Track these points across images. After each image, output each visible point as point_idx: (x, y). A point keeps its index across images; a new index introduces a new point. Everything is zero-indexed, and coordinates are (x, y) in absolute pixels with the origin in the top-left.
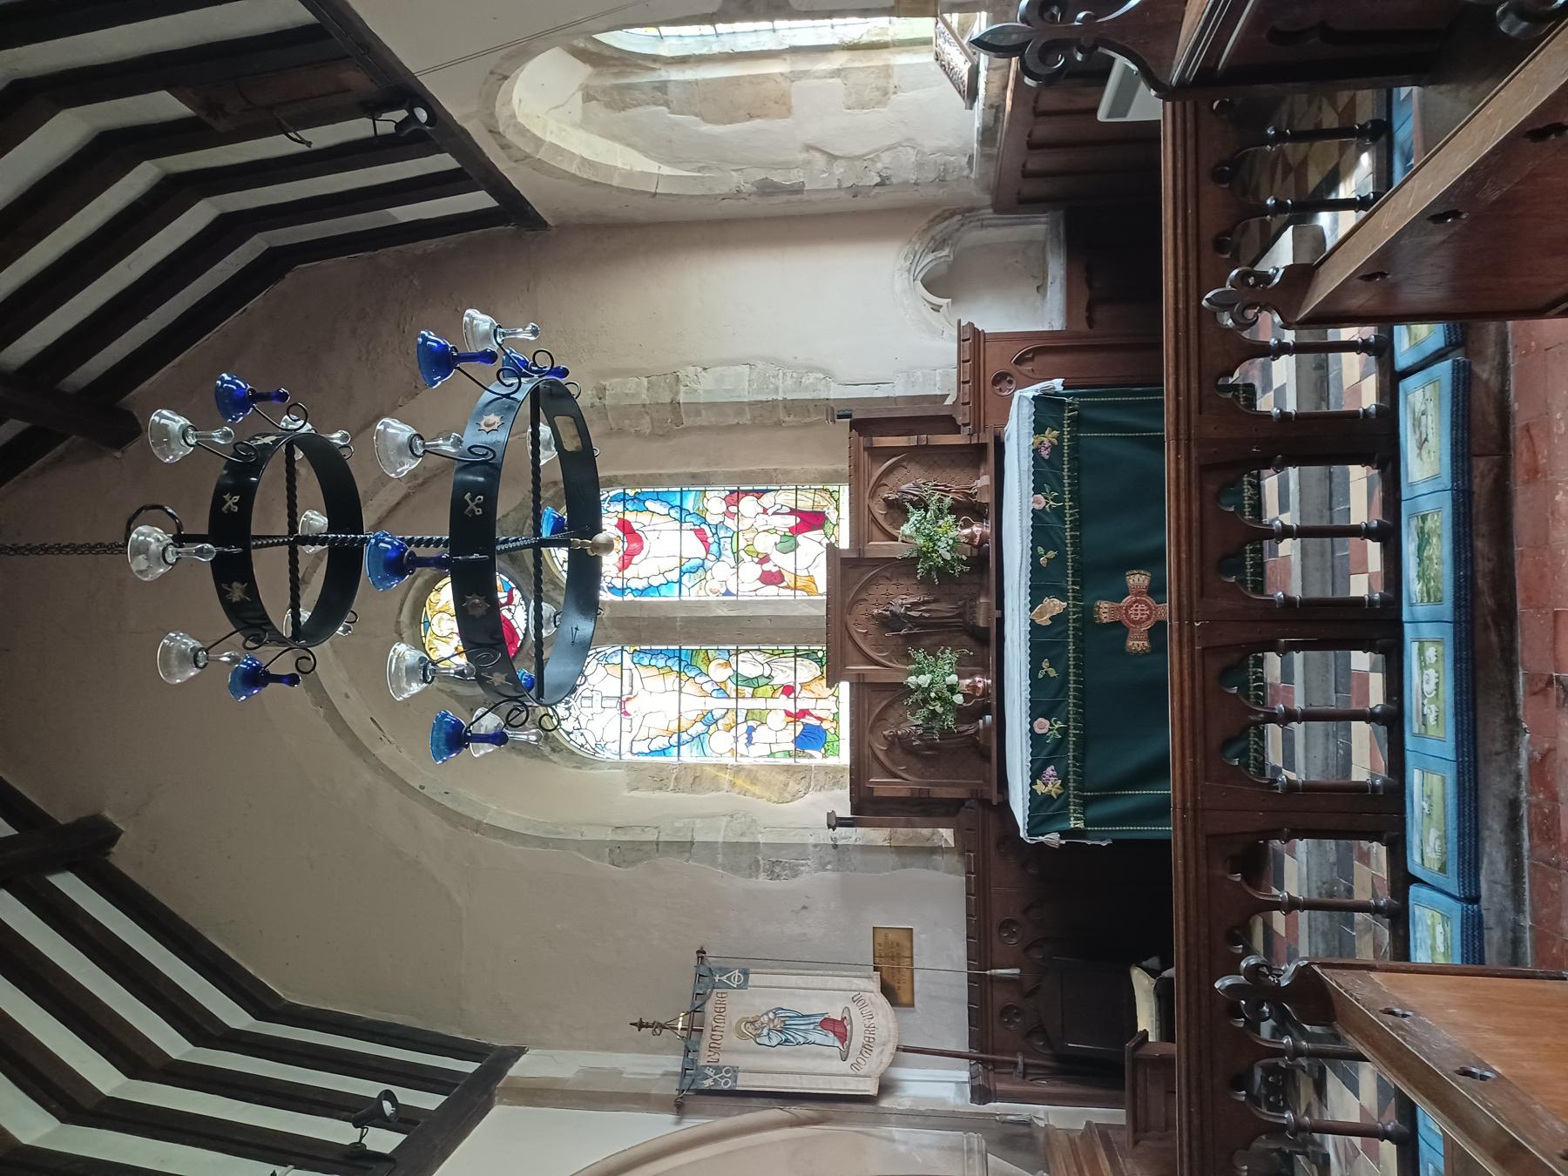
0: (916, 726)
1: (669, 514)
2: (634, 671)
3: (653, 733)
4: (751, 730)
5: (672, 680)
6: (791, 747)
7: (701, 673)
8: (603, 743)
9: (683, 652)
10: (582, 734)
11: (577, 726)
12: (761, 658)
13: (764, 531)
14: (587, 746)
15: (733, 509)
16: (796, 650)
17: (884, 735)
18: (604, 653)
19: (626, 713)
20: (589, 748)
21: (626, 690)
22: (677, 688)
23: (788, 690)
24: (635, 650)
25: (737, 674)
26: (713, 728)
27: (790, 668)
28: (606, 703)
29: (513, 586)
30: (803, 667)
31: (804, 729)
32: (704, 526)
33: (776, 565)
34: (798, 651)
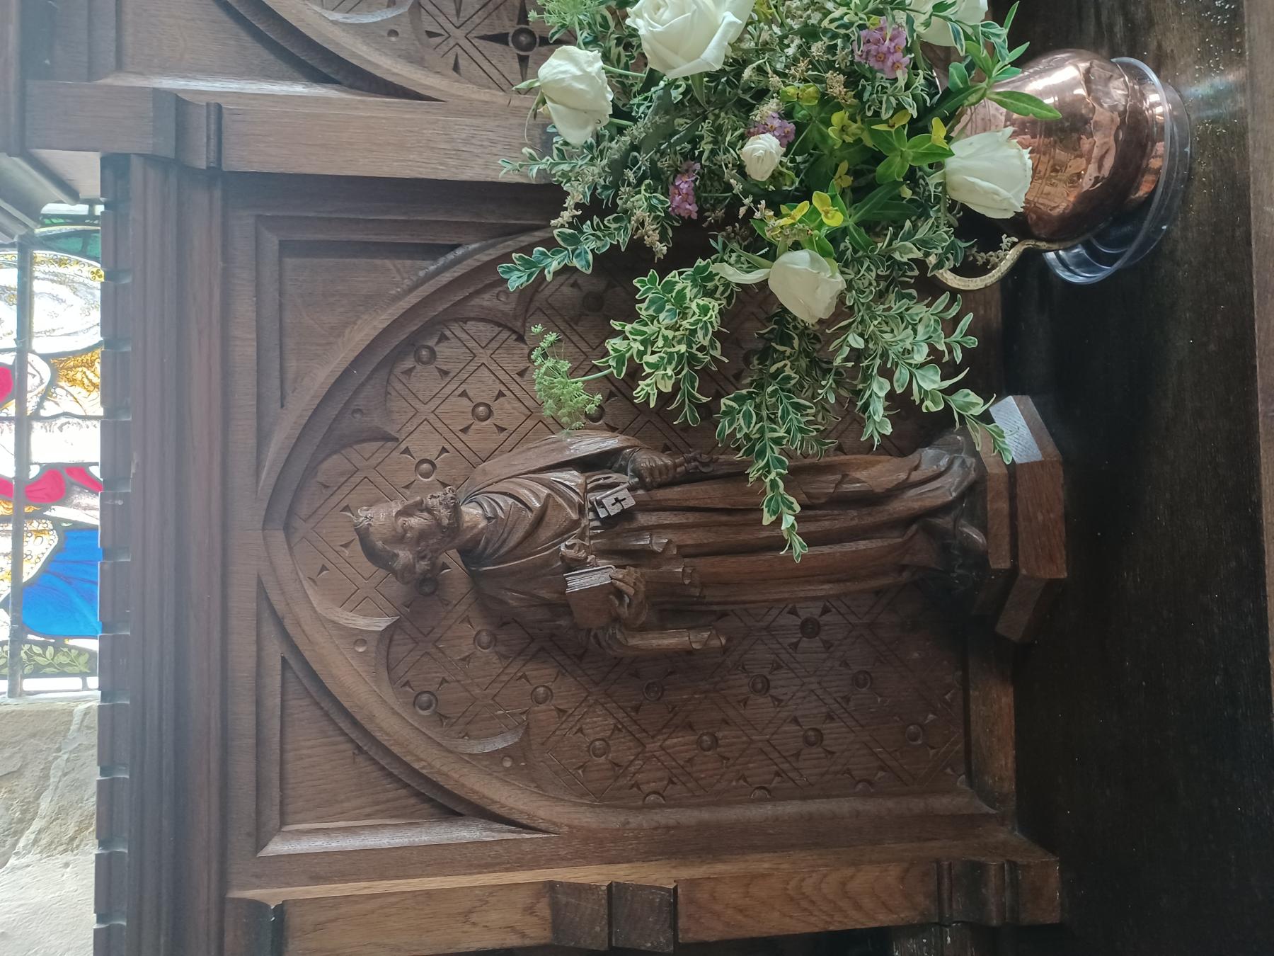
0: (585, 464)
17: (363, 535)
30: (63, 291)
31: (56, 551)
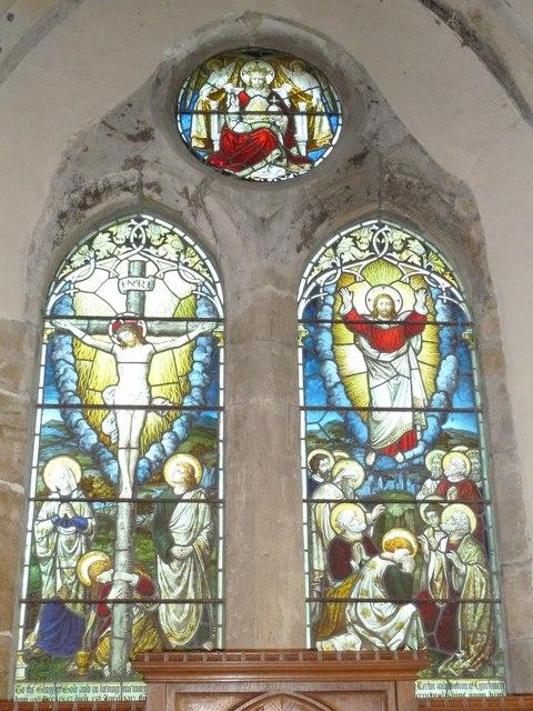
1: (437, 390)
2: (184, 339)
3: (84, 365)
4: (80, 525)
5: (162, 395)
6: (47, 592)
7: (178, 443)
8: (72, 292)
9: (214, 415)
10: (87, 262)
11: (100, 255)
12: (203, 538)
13: (420, 546)
14: (68, 270)
15: (452, 493)
16: (216, 602)
18: (214, 293)
19: (116, 328)
20: (65, 272)
21: (154, 326)
22: (158, 402)
23: (146, 591)
24: (218, 340)
25: (179, 500)
26: (88, 460)
27: (185, 591)
28: (134, 297)
29: (317, 164)
30: (185, 616)
32: (419, 449)
33: (361, 565)
34: (215, 606)
